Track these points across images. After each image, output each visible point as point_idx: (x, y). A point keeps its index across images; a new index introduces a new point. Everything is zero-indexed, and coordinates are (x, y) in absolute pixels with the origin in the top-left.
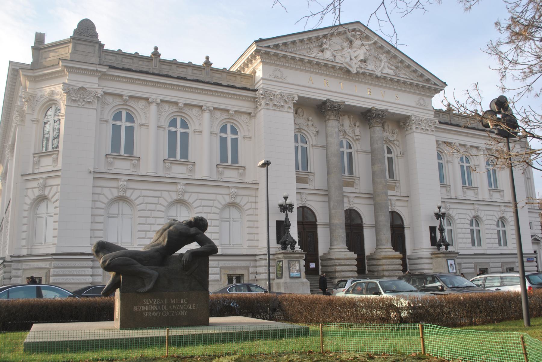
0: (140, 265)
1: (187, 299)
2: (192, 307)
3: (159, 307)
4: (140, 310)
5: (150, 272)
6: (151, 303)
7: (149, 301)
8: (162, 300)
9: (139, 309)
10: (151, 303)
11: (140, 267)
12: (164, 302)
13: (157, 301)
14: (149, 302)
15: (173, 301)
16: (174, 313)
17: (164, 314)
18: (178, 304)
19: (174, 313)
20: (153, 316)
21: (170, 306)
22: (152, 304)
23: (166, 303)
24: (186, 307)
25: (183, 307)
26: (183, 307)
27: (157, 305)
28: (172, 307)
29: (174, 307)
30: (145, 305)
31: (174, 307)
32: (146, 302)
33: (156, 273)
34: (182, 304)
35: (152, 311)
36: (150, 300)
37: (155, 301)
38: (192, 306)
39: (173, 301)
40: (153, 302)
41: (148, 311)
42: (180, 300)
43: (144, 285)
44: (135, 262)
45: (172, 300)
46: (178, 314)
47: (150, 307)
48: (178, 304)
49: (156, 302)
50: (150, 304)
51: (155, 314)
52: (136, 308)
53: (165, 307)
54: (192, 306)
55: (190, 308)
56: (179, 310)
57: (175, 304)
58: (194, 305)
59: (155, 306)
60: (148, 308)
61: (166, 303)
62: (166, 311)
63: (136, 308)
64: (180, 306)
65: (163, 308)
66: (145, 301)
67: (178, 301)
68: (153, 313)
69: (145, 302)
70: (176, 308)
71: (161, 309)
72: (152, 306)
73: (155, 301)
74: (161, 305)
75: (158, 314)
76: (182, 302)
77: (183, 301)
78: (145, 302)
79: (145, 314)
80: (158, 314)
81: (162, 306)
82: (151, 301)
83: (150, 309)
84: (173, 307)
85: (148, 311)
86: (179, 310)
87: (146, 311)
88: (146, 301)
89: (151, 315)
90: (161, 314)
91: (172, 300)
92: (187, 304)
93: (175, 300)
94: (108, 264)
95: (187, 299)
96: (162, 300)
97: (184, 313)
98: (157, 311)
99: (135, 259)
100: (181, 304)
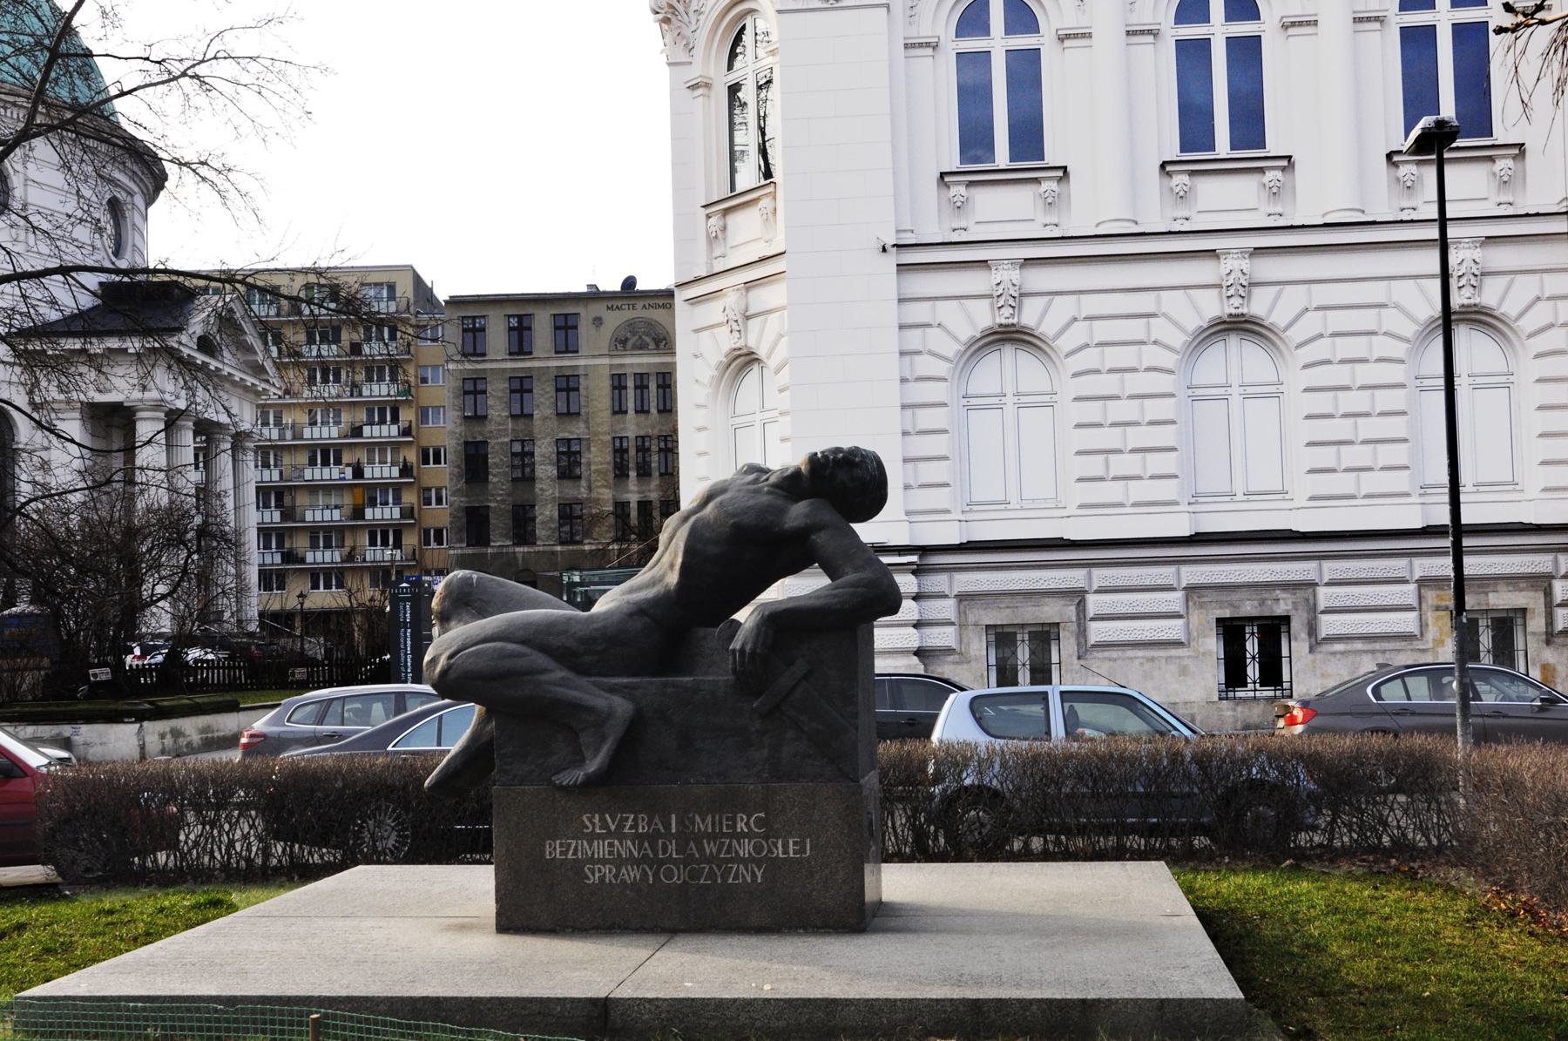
0: (560, 674)
1: (762, 815)
2: (785, 849)
3: (646, 844)
4: (569, 856)
5: (600, 701)
6: (613, 827)
7: (603, 820)
8: (657, 820)
9: (567, 851)
10: (613, 827)
11: (558, 680)
12: (667, 826)
13: (635, 820)
14: (604, 825)
15: (703, 821)
16: (712, 875)
17: (669, 875)
18: (724, 835)
19: (712, 875)
20: (623, 881)
21: (692, 844)
23: (674, 831)
25: (745, 849)
26: (745, 849)
27: (638, 838)
28: (701, 849)
29: (709, 848)
30: (591, 838)
31: (709, 848)
32: (593, 824)
33: (622, 706)
34: (743, 835)
35: (619, 862)
36: (607, 816)
38: (785, 846)
39: (702, 824)
40: (620, 826)
41: (604, 862)
42: (734, 820)
43: (580, 761)
44: (541, 660)
45: (698, 819)
46: (725, 878)
47: (611, 845)
48: (724, 835)
49: (635, 826)
50: (610, 834)
51: (631, 874)
52: (553, 850)
53: (672, 847)
54: (785, 846)
55: (779, 852)
57: (712, 837)
58: (795, 843)
59: (629, 843)
60: (601, 849)
61: (674, 831)
62: (675, 862)
63: (553, 850)
64: (735, 842)
65: (665, 851)
66: (590, 820)
67: (725, 823)
68: (624, 870)
69: (588, 823)
70: (719, 851)
71: (655, 853)
72: (616, 842)
73: (630, 823)
74: (652, 838)
75: (645, 874)
76: (741, 826)
77: (747, 824)
78: (588, 823)
79: (593, 875)
80: (645, 874)
81: (660, 842)
83: (610, 853)
84: (705, 850)
85: (604, 862)
86: (731, 860)
87: (592, 860)
88: (592, 822)
89: (616, 877)
90: (656, 875)
91: (698, 819)
92: (766, 838)
93: (709, 818)
94: (444, 673)
95: (762, 815)
96: (657, 820)
98: (637, 862)
99: (545, 649)
100: (739, 836)
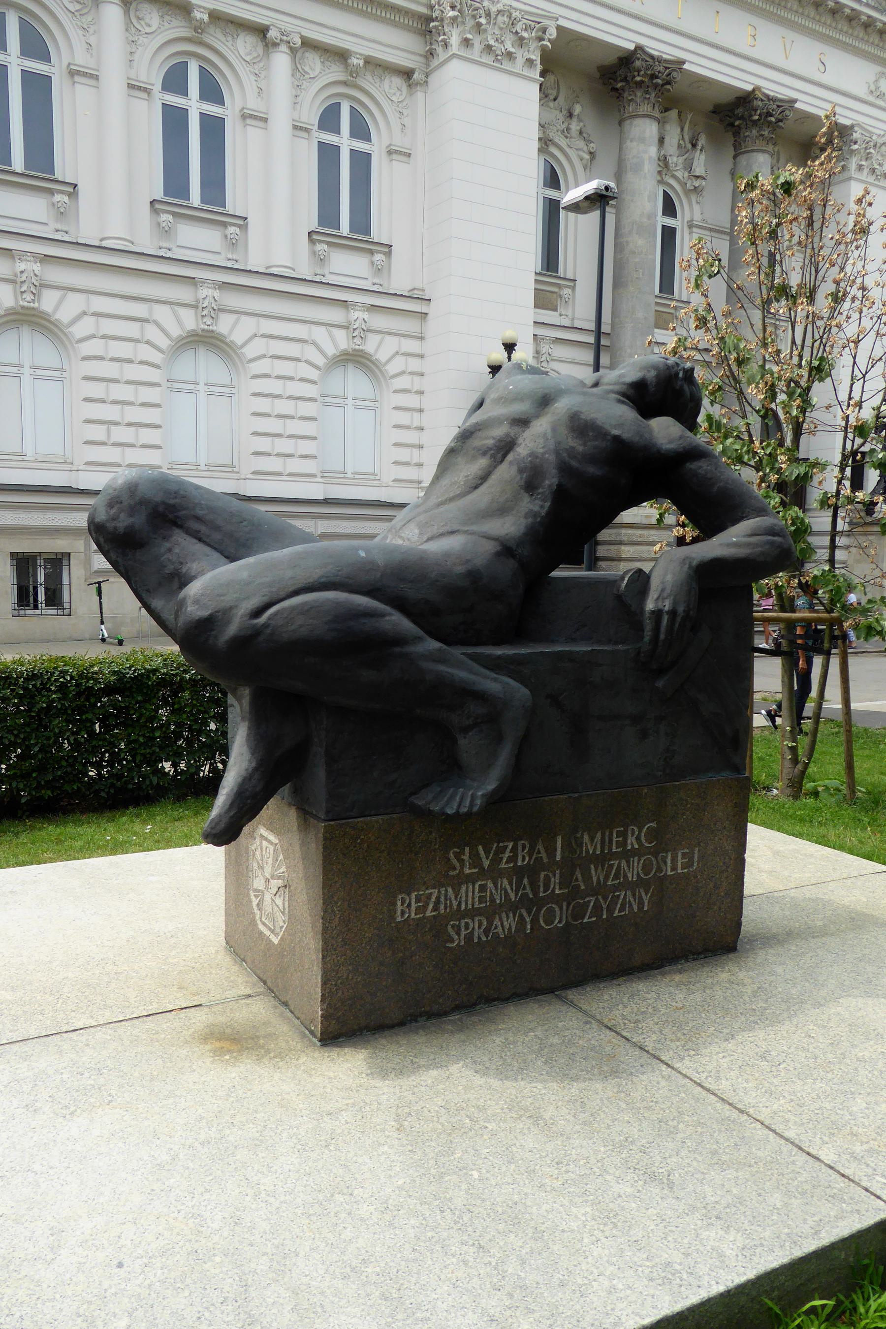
6: (486, 863)
8: (540, 846)
10: (486, 863)
13: (514, 849)
18: (613, 856)
22: (494, 874)
23: (558, 858)
24: (646, 869)
26: (634, 870)
27: (519, 872)
28: (587, 877)
29: (596, 875)
34: (634, 853)
37: (507, 854)
38: (674, 860)
40: (496, 861)
42: (624, 835)
48: (613, 856)
49: (513, 859)
56: (616, 888)
58: (684, 855)
59: (505, 882)
61: (558, 858)
64: (624, 864)
65: (546, 887)
70: (607, 878)
73: (507, 854)
74: (532, 872)
78: (455, 861)
82: (487, 853)
96: (540, 846)
97: (641, 903)
